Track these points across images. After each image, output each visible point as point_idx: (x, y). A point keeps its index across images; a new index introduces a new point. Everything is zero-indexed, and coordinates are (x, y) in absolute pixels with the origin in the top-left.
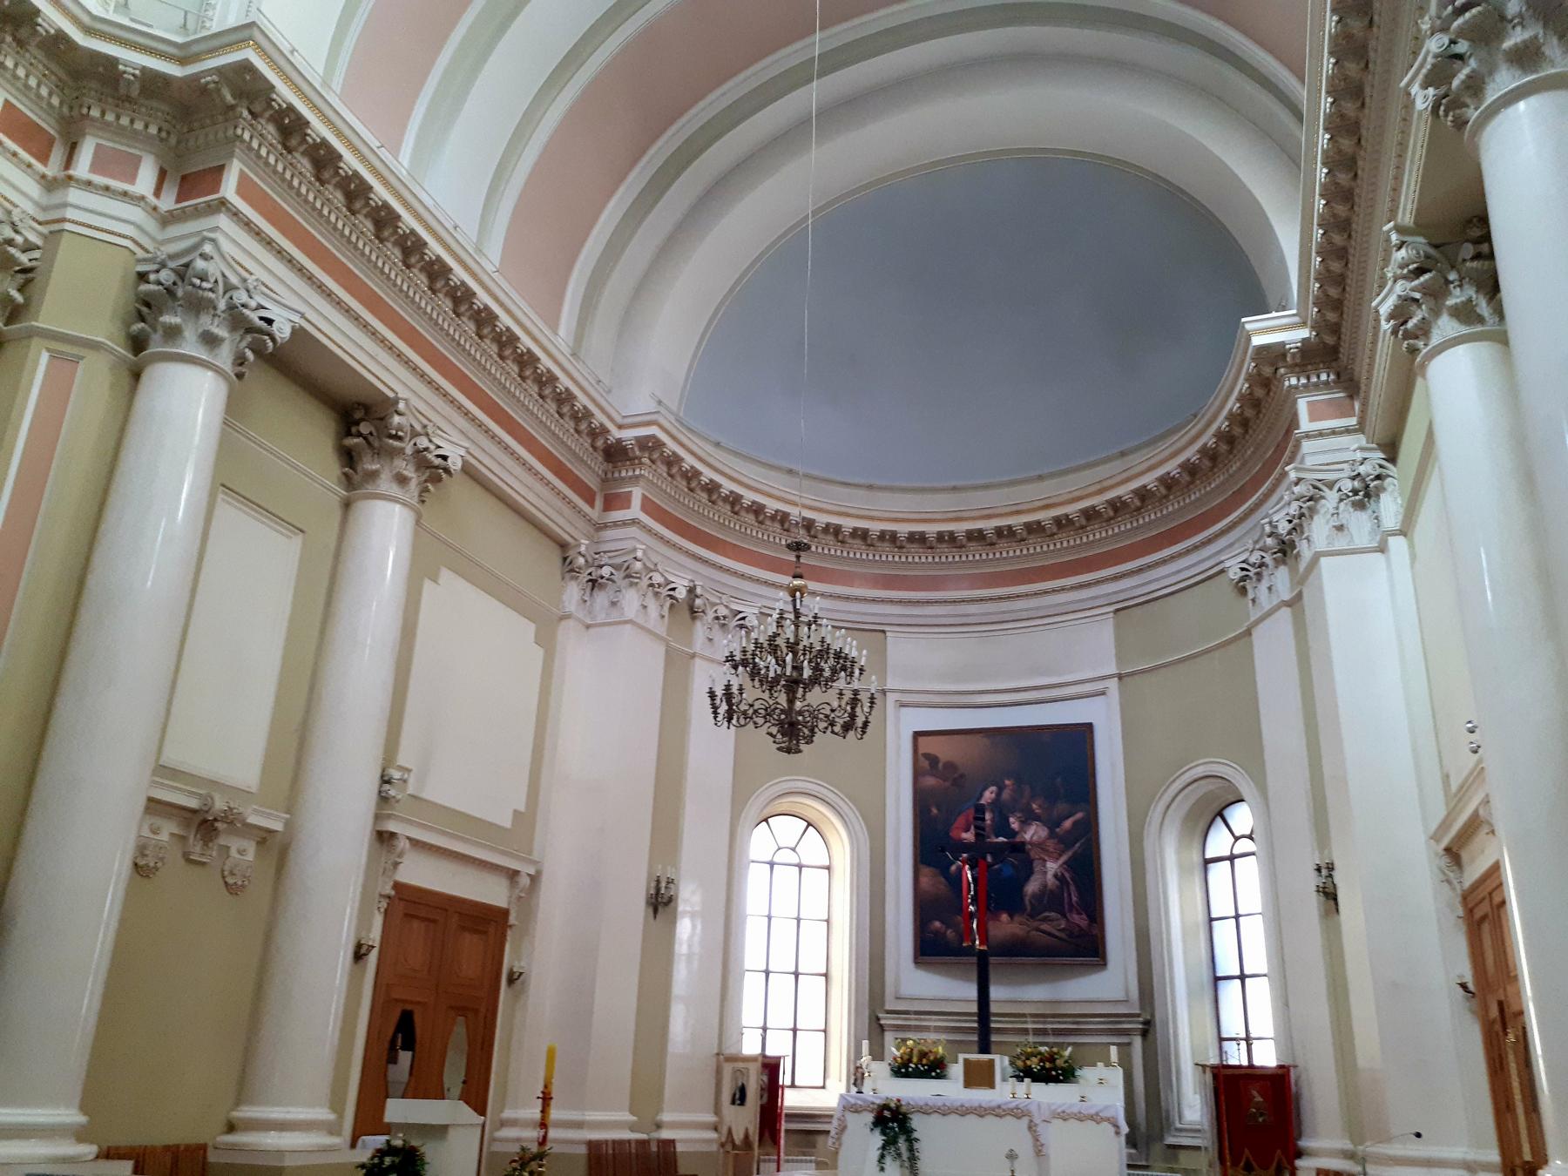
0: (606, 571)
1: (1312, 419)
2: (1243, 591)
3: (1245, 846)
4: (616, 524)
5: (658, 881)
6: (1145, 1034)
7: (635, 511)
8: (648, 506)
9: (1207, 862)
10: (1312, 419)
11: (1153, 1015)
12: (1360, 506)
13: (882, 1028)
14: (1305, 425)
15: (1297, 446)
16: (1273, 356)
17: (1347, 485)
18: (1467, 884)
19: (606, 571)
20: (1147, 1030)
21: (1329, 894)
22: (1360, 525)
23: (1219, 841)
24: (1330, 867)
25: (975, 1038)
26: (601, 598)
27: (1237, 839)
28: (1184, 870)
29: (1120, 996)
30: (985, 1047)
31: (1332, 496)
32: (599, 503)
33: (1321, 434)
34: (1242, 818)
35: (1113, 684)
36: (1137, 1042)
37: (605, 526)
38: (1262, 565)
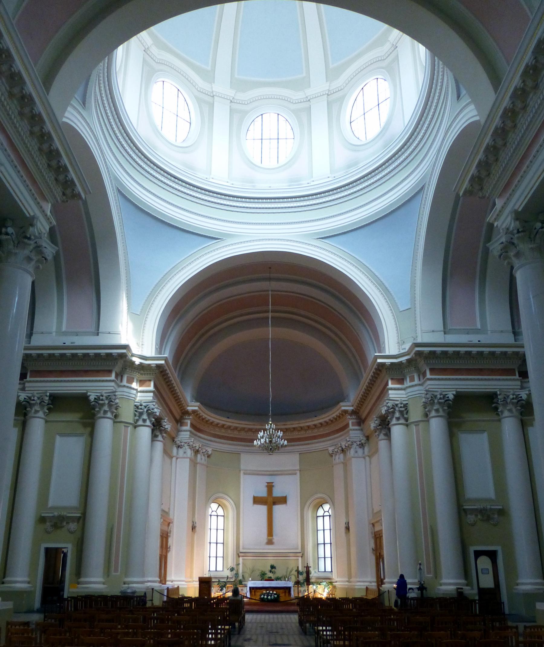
1: (352, 426)
2: (332, 456)
3: (327, 514)
4: (184, 431)
6: (302, 557)
7: (188, 427)
9: (317, 517)
10: (352, 426)
12: (361, 447)
13: (239, 556)
14: (351, 427)
15: (348, 432)
16: (346, 412)
17: (358, 443)
22: (360, 451)
24: (348, 523)
28: (313, 517)
31: (355, 444)
32: (179, 425)
33: (354, 430)
34: (327, 507)
35: (298, 472)
36: (300, 559)
38: (337, 452)
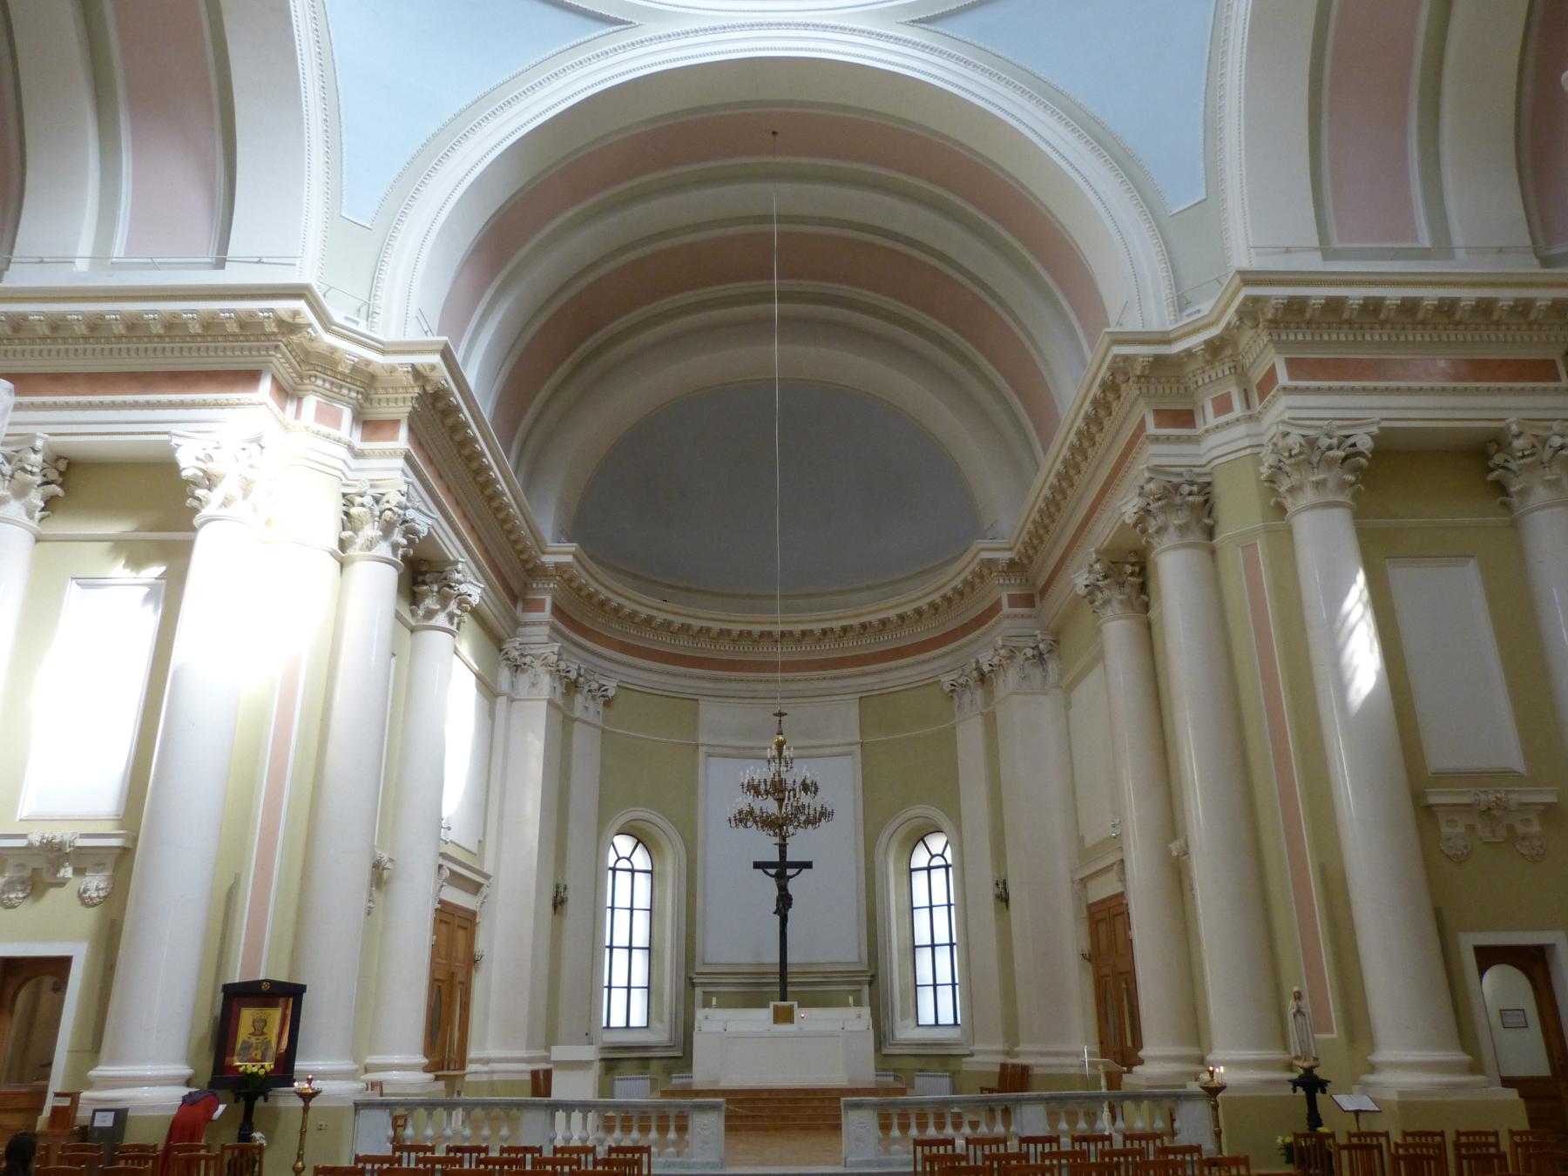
0: (528, 660)
3: (938, 861)
4: (534, 624)
5: (557, 887)
7: (546, 615)
8: (557, 611)
9: (912, 870)
11: (877, 969)
18: (1091, 901)
19: (528, 660)
20: (872, 981)
21: (1003, 898)
23: (920, 858)
24: (1005, 883)
25: (778, 989)
26: (524, 680)
27: (933, 856)
29: (855, 959)
30: (784, 998)
34: (937, 843)
36: (866, 988)
37: (526, 624)
